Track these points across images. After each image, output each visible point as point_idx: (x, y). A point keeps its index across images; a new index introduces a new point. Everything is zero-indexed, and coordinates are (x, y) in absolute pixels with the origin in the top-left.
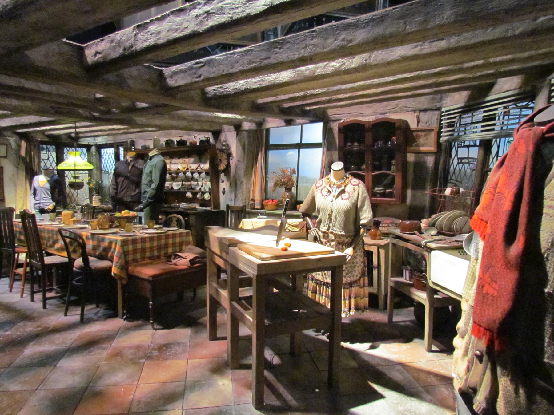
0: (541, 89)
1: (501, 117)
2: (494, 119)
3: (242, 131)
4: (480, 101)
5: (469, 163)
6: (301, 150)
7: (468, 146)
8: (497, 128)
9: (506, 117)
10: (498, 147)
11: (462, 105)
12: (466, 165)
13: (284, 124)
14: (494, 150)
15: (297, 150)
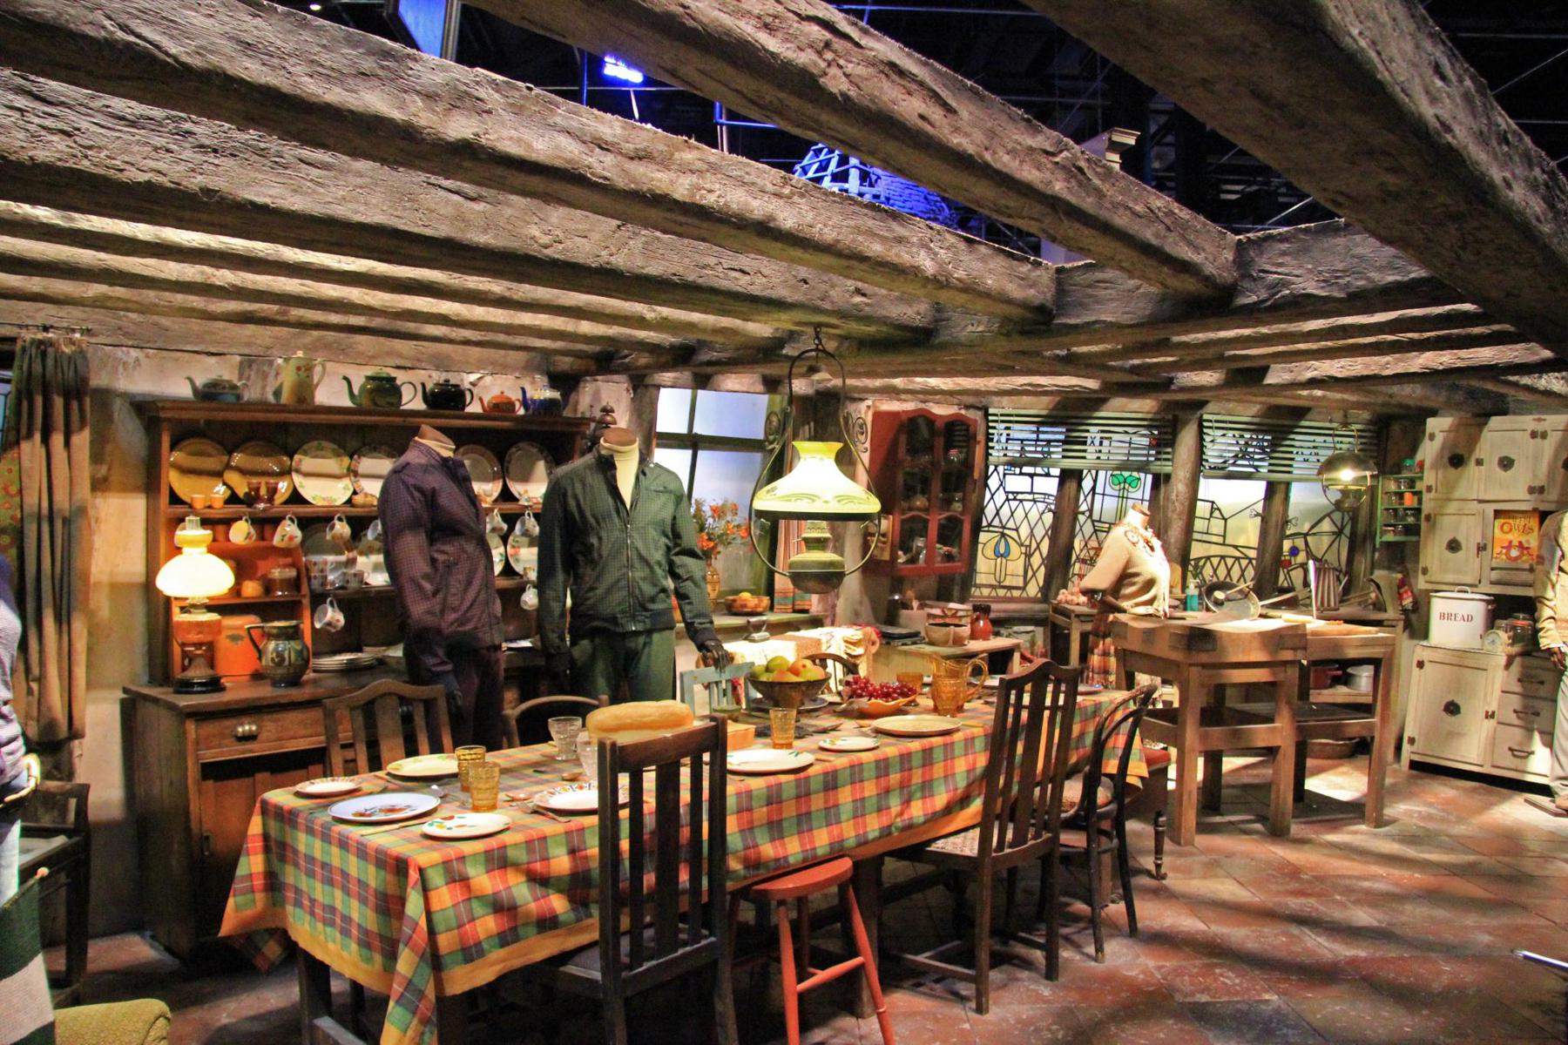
0: (1186, 423)
1: (1097, 442)
2: (1085, 443)
3: (646, 386)
4: (1086, 414)
5: (1035, 501)
6: (700, 453)
7: (1032, 476)
8: (1091, 456)
9: (1106, 443)
10: (1095, 481)
11: (1044, 412)
12: (1028, 505)
13: (760, 388)
14: (1087, 484)
15: (689, 453)
